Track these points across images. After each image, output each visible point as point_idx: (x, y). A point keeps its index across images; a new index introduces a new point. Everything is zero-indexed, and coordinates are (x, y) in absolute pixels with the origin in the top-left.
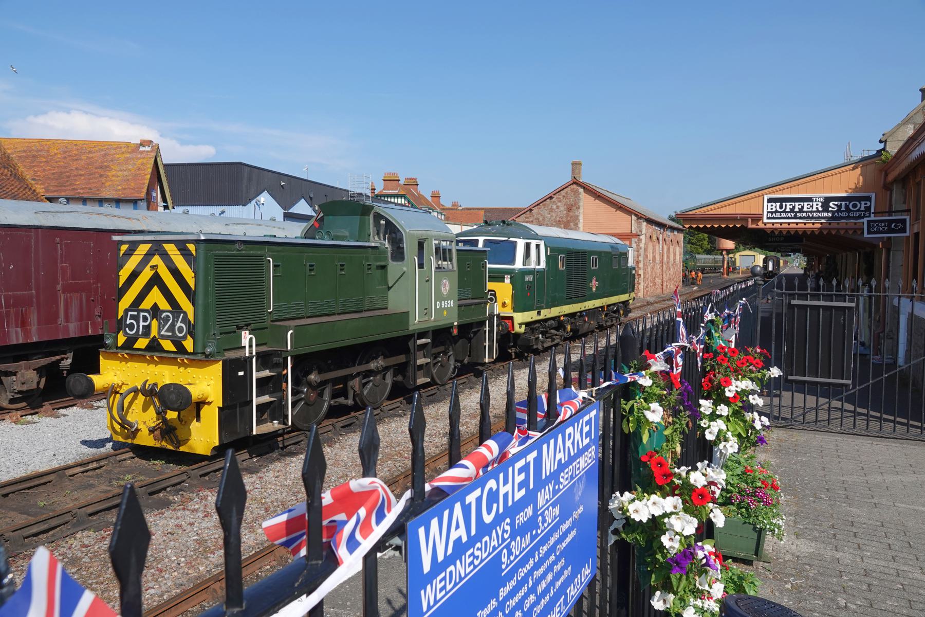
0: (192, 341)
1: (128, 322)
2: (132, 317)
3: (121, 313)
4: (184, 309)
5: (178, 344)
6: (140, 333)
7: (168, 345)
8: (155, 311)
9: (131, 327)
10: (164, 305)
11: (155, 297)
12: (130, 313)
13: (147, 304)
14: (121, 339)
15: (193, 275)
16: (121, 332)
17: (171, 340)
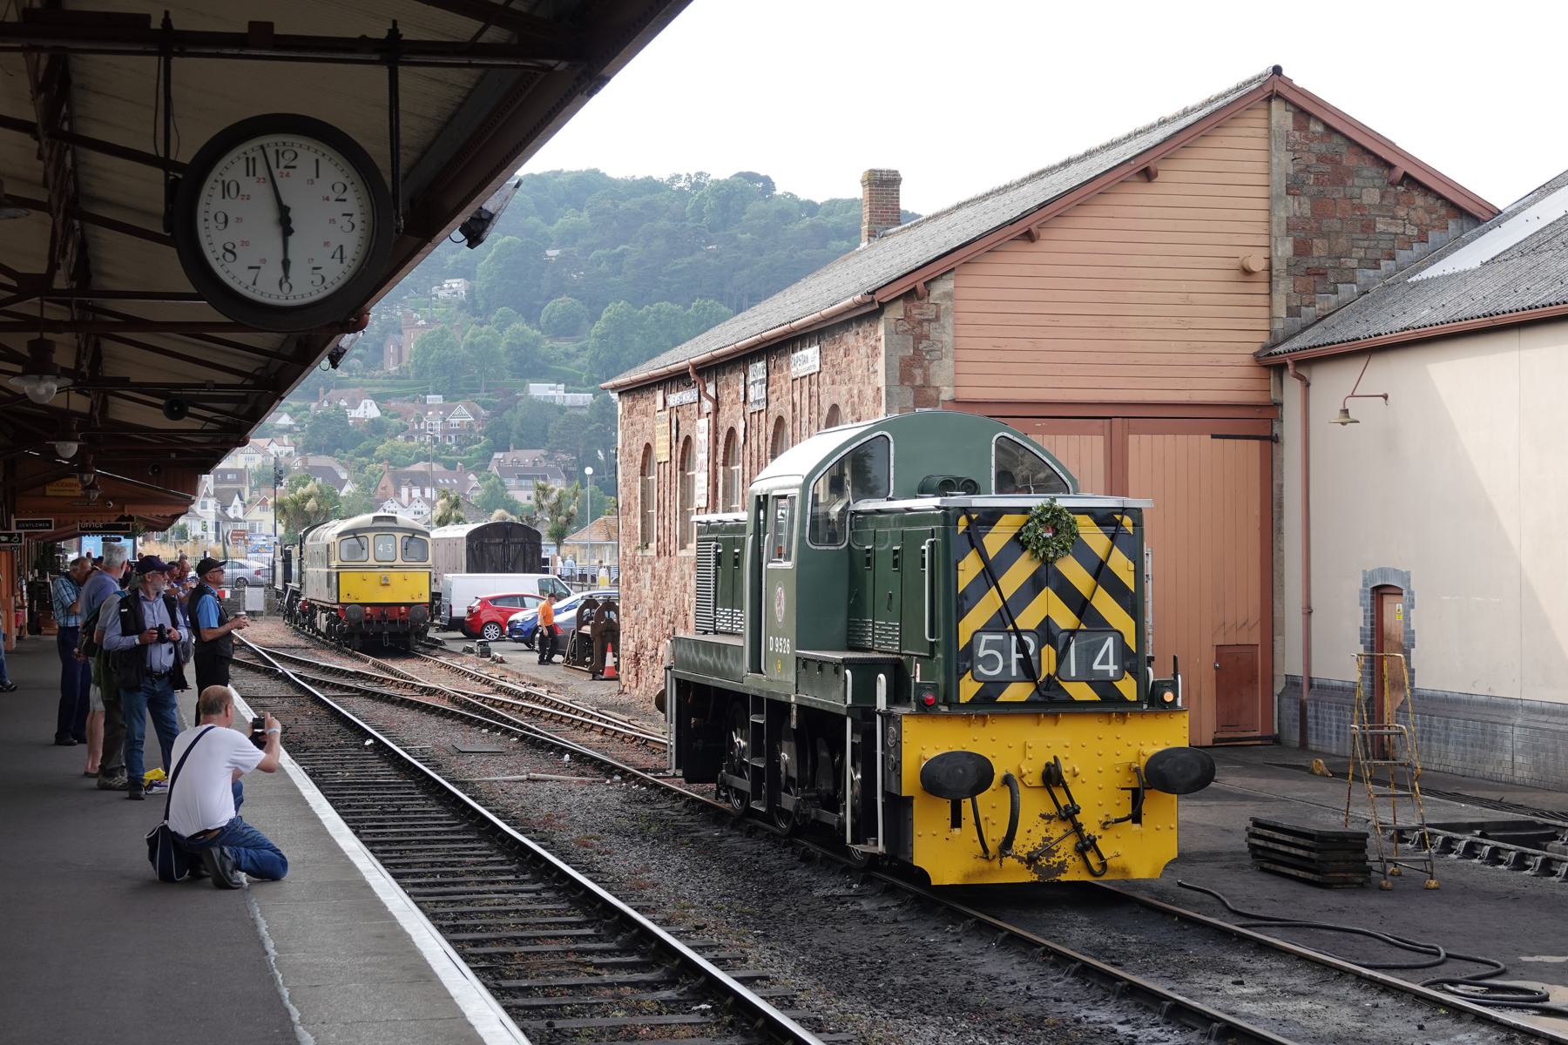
0: (1134, 683)
1: (982, 653)
2: (989, 645)
3: (963, 640)
4: (1115, 627)
5: (1105, 687)
6: (1014, 673)
7: (1081, 692)
8: (1046, 632)
9: (990, 661)
10: (1065, 619)
11: (1048, 606)
12: (985, 637)
13: (1028, 619)
14: (968, 689)
15: (1132, 566)
16: (968, 675)
17: (1087, 682)
